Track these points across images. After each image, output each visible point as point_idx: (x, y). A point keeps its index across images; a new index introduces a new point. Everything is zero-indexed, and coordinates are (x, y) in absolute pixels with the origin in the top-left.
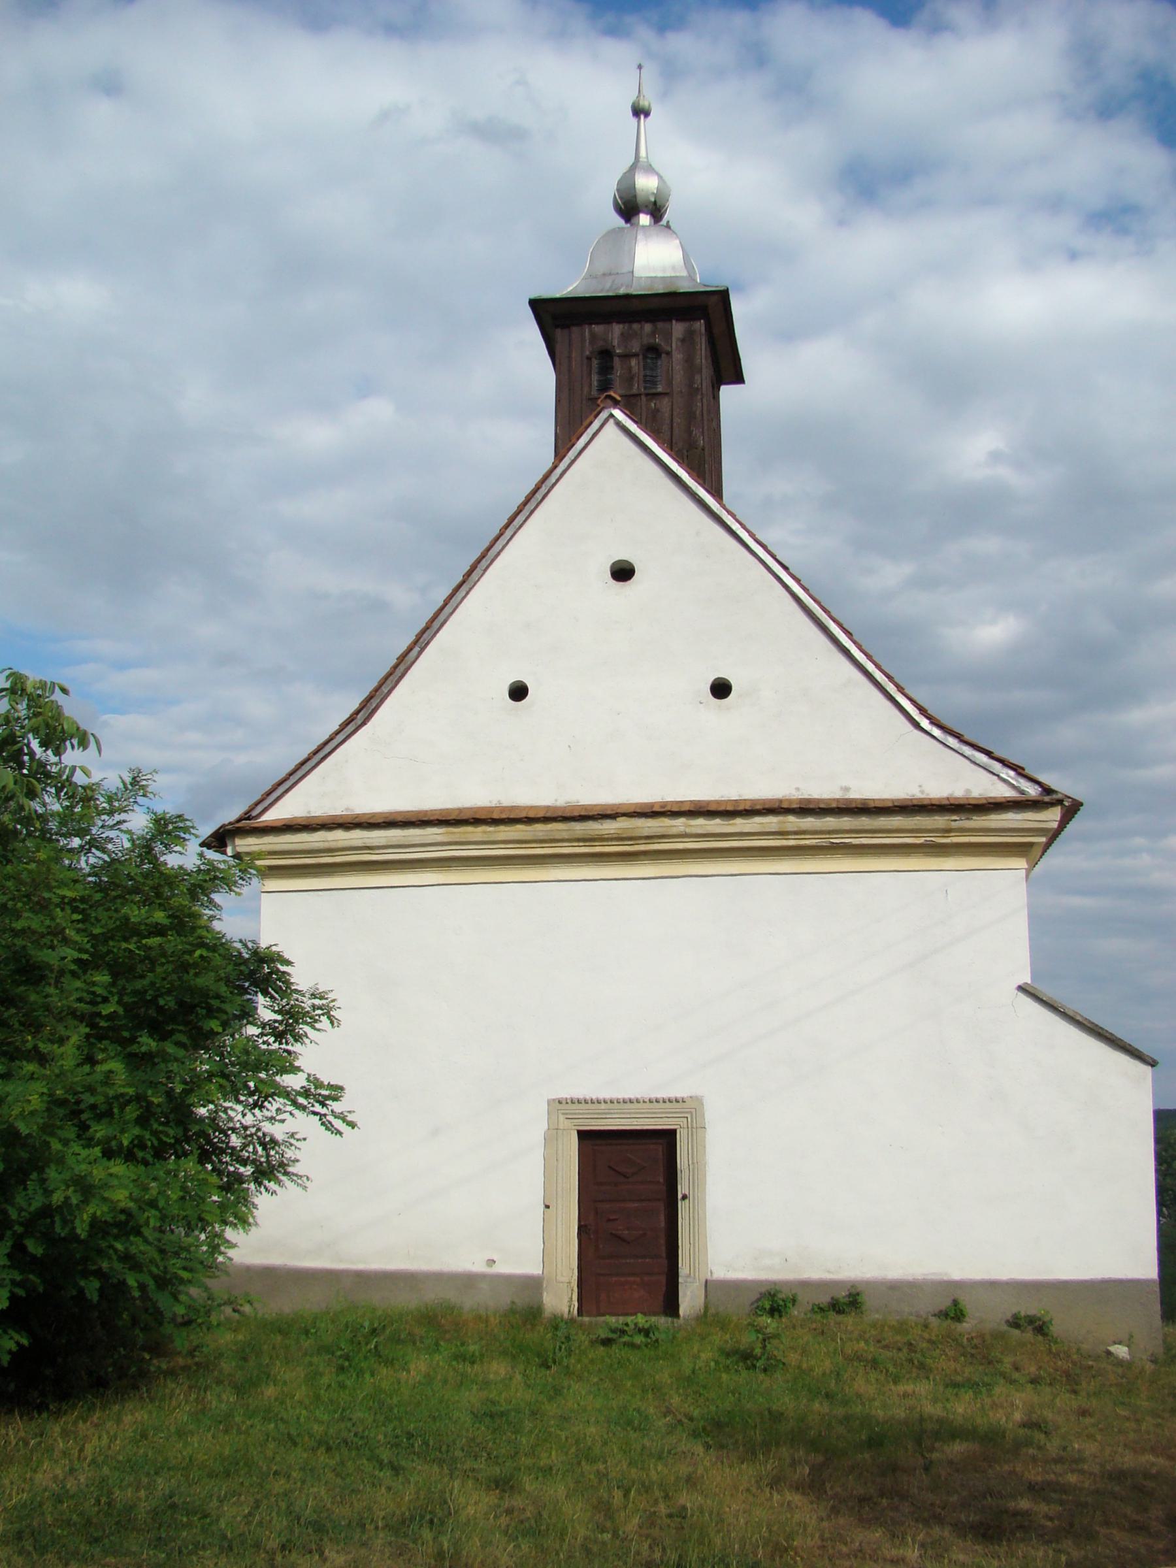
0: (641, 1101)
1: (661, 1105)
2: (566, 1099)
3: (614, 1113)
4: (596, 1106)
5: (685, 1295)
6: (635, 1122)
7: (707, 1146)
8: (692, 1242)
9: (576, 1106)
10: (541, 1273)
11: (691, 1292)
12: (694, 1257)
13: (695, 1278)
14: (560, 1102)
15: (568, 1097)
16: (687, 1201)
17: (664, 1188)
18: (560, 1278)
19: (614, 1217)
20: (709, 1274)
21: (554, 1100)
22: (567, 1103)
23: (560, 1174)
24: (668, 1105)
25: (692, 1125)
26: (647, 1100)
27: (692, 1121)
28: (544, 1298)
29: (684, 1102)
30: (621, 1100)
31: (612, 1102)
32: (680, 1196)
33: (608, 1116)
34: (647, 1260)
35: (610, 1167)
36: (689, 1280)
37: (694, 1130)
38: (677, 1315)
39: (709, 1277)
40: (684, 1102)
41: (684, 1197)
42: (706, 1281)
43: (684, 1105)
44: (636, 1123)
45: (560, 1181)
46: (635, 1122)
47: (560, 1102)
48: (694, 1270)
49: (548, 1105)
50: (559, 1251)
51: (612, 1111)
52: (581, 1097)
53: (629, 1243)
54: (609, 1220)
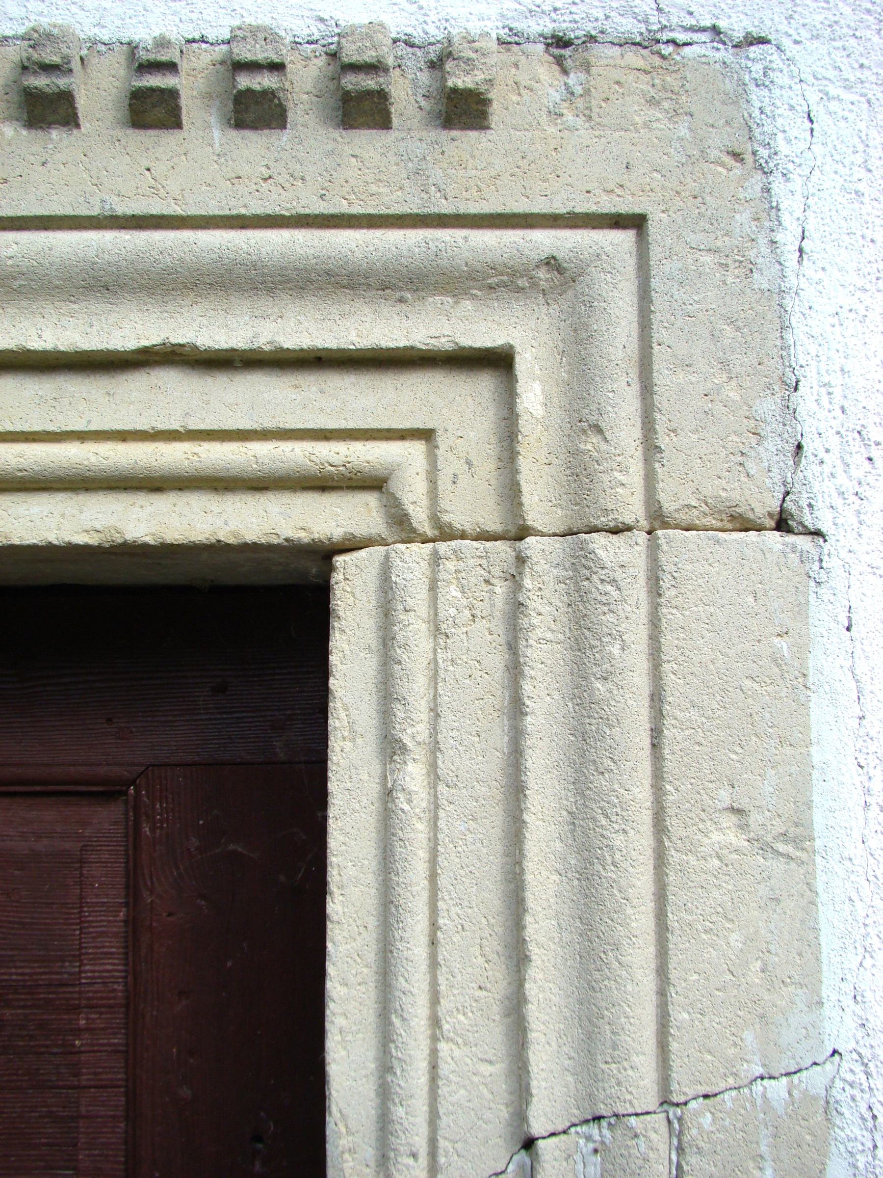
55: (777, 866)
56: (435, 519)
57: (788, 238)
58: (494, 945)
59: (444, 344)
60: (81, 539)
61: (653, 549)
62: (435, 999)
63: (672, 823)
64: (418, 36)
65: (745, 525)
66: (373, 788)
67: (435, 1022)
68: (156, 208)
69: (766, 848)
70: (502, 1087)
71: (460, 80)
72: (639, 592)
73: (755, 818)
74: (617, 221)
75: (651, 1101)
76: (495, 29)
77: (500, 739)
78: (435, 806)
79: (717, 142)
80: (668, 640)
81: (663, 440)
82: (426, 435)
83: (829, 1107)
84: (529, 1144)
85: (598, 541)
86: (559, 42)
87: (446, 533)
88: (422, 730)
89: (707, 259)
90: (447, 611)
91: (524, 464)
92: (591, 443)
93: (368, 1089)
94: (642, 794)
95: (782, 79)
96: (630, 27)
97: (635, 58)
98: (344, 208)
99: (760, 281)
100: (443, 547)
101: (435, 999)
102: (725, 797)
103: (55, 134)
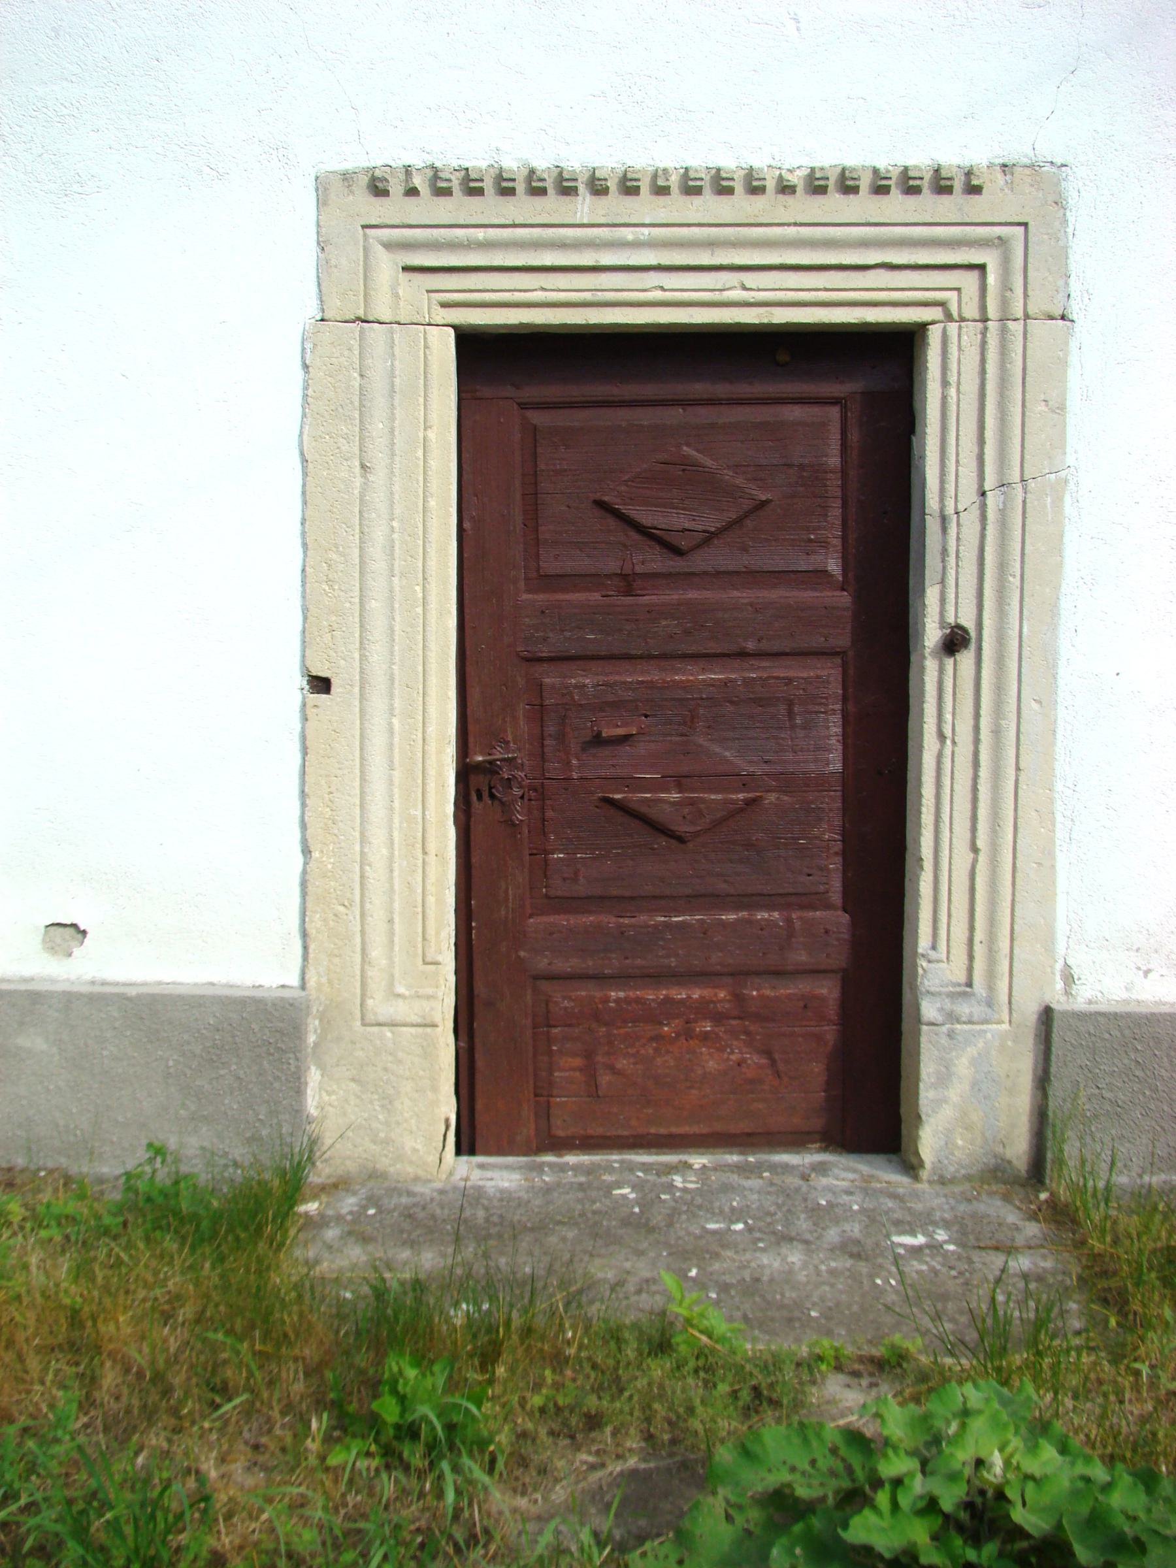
0: (771, 185)
1: (863, 206)
2: (408, 170)
3: (636, 245)
4: (551, 207)
5: (944, 1079)
6: (730, 286)
7: (1074, 402)
8: (980, 844)
9: (458, 208)
10: (294, 980)
11: (974, 1062)
12: (993, 904)
13: (990, 1003)
14: (378, 189)
15: (417, 160)
16: (966, 659)
17: (844, 599)
18: (380, 1007)
19: (621, 731)
20: (1059, 985)
21: (347, 178)
22: (412, 192)
23: (379, 534)
24: (896, 205)
25: (1004, 303)
26: (795, 179)
27: (1006, 286)
28: (312, 1105)
29: (974, 190)
30: (674, 180)
31: (629, 187)
32: (932, 634)
33: (607, 259)
34: (761, 915)
35: (601, 505)
36: (964, 1009)
37: (1016, 327)
38: (912, 1167)
39: (1060, 1003)
40: (974, 190)
41: (954, 642)
42: (1047, 1015)
43: (977, 208)
44: (737, 295)
45: (378, 565)
46: (730, 286)
47: (378, 189)
48: (992, 961)
49: (322, 202)
50: (376, 875)
51: (629, 234)
52: (478, 159)
53: (681, 840)
54: (598, 741)
55: (1055, 416)
56: (960, 315)
57: (1070, 230)
58: (975, 440)
59: (966, 262)
60: (853, 321)
61: (1025, 326)
62: (957, 455)
63: (1027, 404)
64: (962, 165)
65: (1052, 318)
66: (940, 396)
67: (957, 461)
68: (882, 221)
69: (1053, 412)
70: (976, 479)
71: (975, 182)
72: (1021, 338)
73: (1050, 403)
74: (1019, 224)
75: (1017, 479)
76: (985, 163)
77: (977, 381)
78: (959, 400)
79: (1050, 199)
80: (1029, 352)
81: (1030, 293)
82: (958, 290)
83: (1066, 481)
84: (983, 494)
85: (1010, 324)
86: (1005, 166)
87: (963, 320)
88: (955, 378)
89: (1045, 237)
90: (963, 343)
91: (988, 299)
92: (1008, 294)
93: (937, 481)
94: (1019, 396)
95: (1071, 178)
96: (1026, 161)
97: (1028, 171)
98: (938, 220)
99: (1061, 243)
100: (963, 324)
101: (957, 455)
102: (1042, 397)
103: (851, 196)
